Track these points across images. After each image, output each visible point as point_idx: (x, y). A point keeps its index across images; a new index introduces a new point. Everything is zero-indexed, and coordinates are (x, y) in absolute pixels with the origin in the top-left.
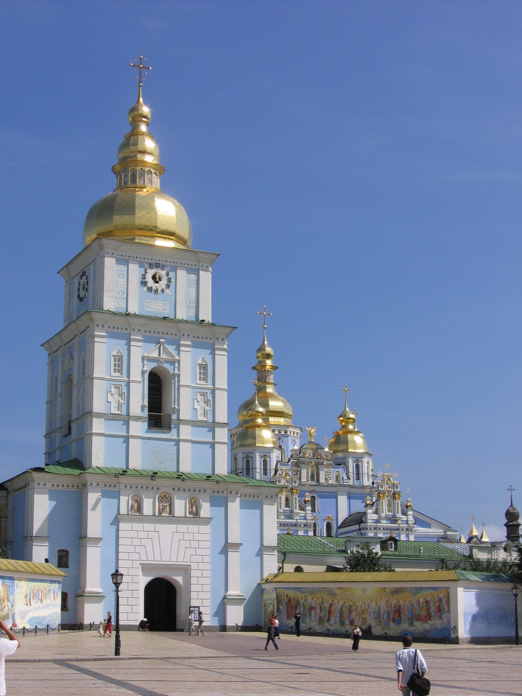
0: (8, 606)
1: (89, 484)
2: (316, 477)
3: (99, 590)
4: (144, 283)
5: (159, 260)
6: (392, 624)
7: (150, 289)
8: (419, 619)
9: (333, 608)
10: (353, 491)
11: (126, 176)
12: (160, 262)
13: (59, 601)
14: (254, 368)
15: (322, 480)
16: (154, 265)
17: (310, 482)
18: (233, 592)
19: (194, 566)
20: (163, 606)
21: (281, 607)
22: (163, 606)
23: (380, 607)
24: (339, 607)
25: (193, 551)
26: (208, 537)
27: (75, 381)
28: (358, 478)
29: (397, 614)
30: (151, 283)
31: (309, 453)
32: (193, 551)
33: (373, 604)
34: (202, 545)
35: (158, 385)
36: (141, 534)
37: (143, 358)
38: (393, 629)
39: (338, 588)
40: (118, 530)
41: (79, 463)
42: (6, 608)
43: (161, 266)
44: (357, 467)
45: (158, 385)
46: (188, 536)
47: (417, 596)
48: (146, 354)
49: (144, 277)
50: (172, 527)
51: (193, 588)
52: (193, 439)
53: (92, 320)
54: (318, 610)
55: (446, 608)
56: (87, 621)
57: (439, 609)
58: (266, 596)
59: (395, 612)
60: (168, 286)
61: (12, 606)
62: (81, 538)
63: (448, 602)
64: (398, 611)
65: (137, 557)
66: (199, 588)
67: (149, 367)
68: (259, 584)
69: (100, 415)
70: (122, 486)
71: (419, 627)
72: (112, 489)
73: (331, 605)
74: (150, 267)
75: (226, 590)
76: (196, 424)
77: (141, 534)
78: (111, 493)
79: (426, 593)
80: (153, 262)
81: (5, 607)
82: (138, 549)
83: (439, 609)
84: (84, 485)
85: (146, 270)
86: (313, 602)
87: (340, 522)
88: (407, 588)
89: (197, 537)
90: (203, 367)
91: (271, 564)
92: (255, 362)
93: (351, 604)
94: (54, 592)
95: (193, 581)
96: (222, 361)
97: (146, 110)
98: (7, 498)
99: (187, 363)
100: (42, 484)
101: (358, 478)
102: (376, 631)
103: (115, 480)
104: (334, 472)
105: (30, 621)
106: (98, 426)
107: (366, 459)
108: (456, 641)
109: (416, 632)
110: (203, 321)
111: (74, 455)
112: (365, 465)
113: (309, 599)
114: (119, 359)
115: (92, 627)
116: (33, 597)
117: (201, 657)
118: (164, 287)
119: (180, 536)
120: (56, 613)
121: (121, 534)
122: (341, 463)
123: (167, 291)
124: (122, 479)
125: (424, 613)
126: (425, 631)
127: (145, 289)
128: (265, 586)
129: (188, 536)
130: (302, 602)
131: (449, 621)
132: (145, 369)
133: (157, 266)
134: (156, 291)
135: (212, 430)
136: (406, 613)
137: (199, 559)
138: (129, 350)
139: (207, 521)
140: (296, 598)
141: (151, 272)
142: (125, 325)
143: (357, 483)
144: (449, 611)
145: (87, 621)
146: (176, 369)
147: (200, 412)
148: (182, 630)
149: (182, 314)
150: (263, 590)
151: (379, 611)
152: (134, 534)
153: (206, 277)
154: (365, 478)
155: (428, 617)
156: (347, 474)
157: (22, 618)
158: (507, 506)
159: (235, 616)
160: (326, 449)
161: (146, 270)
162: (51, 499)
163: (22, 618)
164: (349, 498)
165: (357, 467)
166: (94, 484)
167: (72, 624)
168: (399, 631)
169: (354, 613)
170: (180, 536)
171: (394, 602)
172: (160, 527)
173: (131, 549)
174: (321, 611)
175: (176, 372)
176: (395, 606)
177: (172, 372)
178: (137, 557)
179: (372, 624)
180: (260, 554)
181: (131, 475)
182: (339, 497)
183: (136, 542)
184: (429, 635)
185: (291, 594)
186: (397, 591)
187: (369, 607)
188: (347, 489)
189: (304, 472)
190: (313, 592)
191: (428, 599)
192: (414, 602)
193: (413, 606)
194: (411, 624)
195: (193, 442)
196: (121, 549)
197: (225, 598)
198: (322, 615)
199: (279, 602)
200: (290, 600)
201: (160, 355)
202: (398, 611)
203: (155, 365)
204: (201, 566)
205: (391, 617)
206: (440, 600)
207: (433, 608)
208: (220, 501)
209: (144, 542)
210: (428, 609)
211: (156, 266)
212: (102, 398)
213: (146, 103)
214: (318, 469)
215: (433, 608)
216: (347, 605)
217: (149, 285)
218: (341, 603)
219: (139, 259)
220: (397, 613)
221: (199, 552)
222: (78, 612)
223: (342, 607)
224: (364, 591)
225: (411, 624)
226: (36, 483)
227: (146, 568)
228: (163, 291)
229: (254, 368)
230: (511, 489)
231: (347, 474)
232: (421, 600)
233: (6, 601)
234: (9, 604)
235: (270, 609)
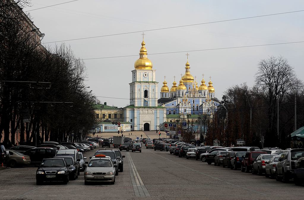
13: (130, 127)
15: (196, 97)
18: (158, 125)
28: (204, 96)
30: (145, 76)
35: (146, 92)
45: (146, 92)
56: (135, 130)
87: (200, 105)
101: (204, 96)
104: (199, 94)
145: (135, 130)
147: (153, 96)
157: (124, 130)
159: (158, 128)
163: (124, 130)
165: (204, 93)
167: (133, 130)
188: (202, 98)
212: (137, 96)
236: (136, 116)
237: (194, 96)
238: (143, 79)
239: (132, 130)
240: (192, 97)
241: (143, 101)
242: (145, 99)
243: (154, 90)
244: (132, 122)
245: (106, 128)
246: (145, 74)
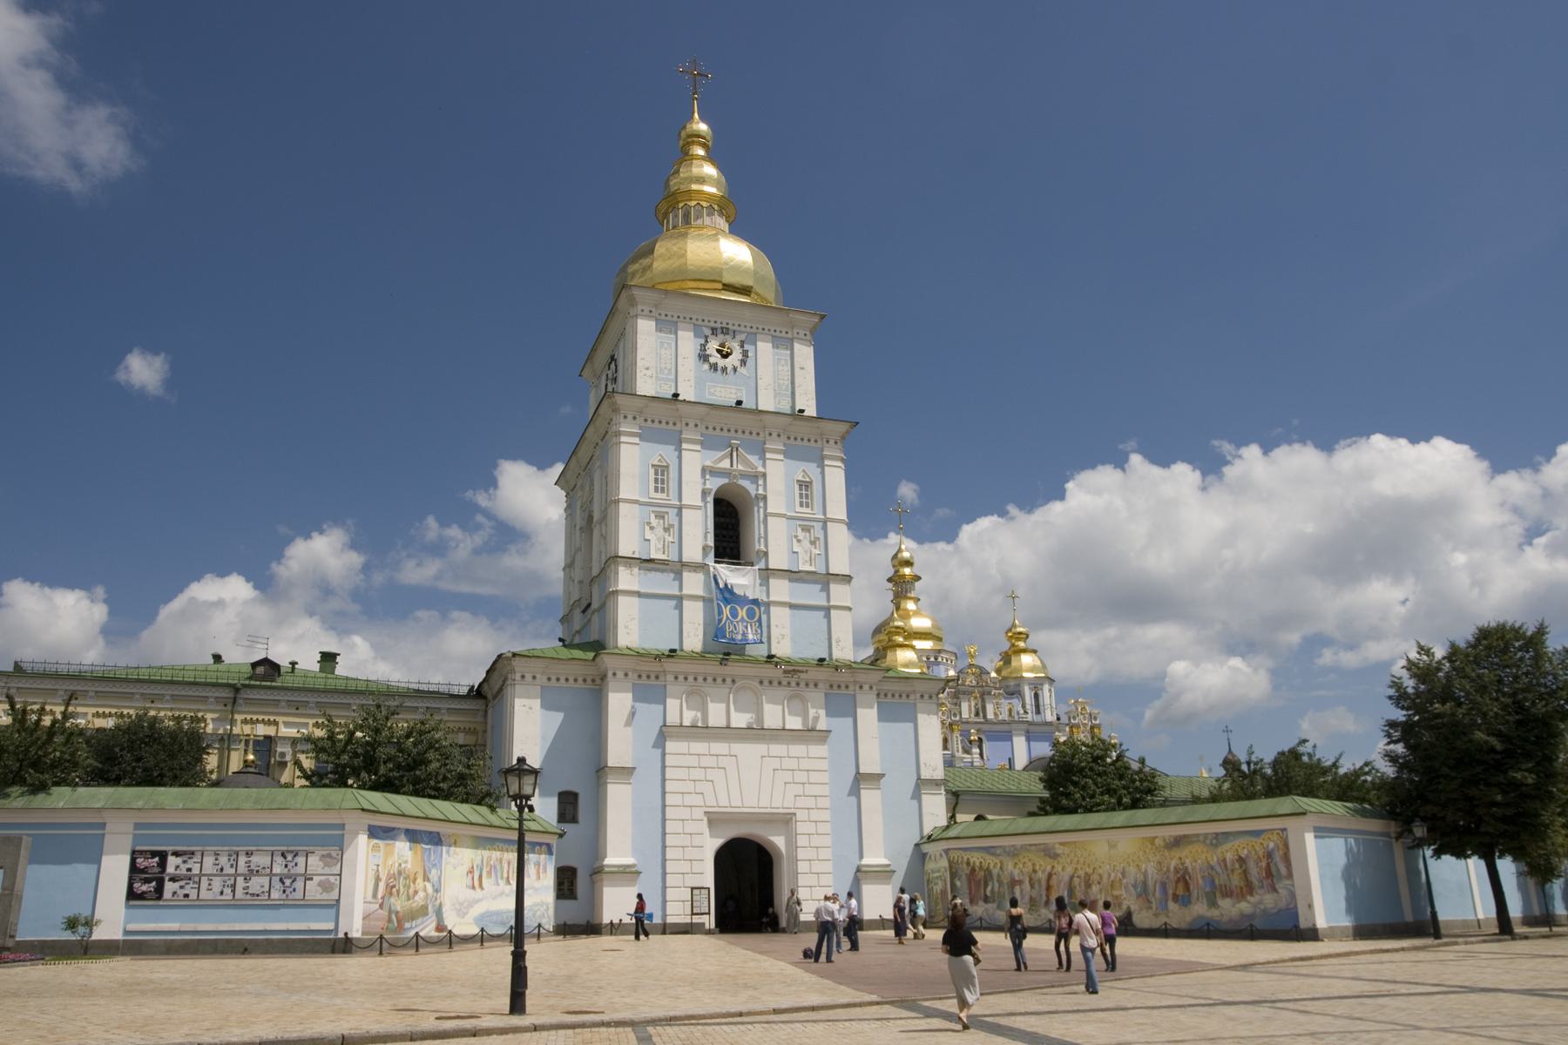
0: (425, 890)
1: (610, 674)
2: (980, 711)
3: (629, 861)
4: (704, 357)
6: (1171, 905)
7: (714, 367)
8: (1228, 893)
9: (1054, 882)
10: (1032, 728)
11: (676, 216)
14: (889, 580)
15: (990, 716)
17: (974, 719)
19: (801, 815)
20: (747, 887)
21: (958, 883)
22: (747, 887)
23: (1145, 874)
24: (1067, 879)
25: (799, 789)
26: (824, 765)
27: (596, 516)
28: (1038, 712)
29: (1181, 886)
30: (716, 358)
31: (970, 680)
32: (799, 789)
33: (1132, 870)
34: (814, 777)
36: (706, 761)
37: (704, 470)
38: (1177, 916)
39: (1062, 844)
40: (664, 755)
41: (598, 646)
42: (421, 894)
44: (1036, 696)
46: (787, 764)
47: (1220, 850)
48: (708, 463)
49: (703, 347)
50: (761, 748)
51: (801, 854)
52: (794, 601)
53: (616, 410)
54: (1027, 885)
55: (1283, 871)
57: (1269, 874)
58: (930, 866)
59: (1178, 881)
60: (743, 362)
61: (437, 891)
62: (600, 772)
63: (1286, 858)
64: (1183, 878)
65: (698, 800)
66: (811, 854)
67: (714, 484)
68: (917, 845)
69: (630, 561)
70: (670, 678)
71: (1229, 909)
72: (653, 682)
73: (1050, 875)
75: (861, 857)
76: (793, 575)
77: (706, 761)
78: (650, 687)
79: (1236, 843)
80: (718, 325)
81: (416, 892)
82: (700, 787)
83: (1269, 874)
84: (603, 678)
86: (1016, 872)
88: (1197, 835)
89: (805, 764)
90: (805, 485)
91: (935, 810)
92: (891, 572)
93: (1090, 871)
94: (538, 864)
95: (801, 841)
96: (836, 477)
97: (703, 127)
98: (486, 711)
99: (777, 482)
100: (528, 677)
101: (1038, 712)
102: (1142, 919)
103: (655, 667)
104: (1005, 704)
105: (477, 920)
106: (626, 579)
107: (1046, 687)
108: (1312, 935)
109: (1225, 919)
110: (802, 411)
111: (594, 637)
112: (1046, 693)
113: (1010, 866)
114: (661, 470)
115: (614, 929)
116: (489, 873)
117: (776, 1011)
118: (737, 364)
119: (776, 763)
120: (542, 904)
121: (669, 760)
122: (1014, 692)
123: (742, 370)
124: (670, 665)
125: (1236, 881)
126: (1243, 916)
127: (706, 366)
128: (927, 848)
129: (787, 764)
130: (995, 872)
131: (1293, 895)
133: (725, 331)
134: (724, 369)
135: (826, 589)
136: (1198, 883)
137: (810, 802)
138: (680, 457)
139: (823, 736)
140: (985, 865)
141: (713, 346)
142: (670, 418)
143: (1037, 719)
144: (1290, 875)
147: (803, 557)
148: (784, 931)
149: (767, 403)
150: (924, 855)
151: (1145, 883)
152: (693, 761)
153: (805, 354)
154: (1048, 712)
155: (1249, 888)
156: (1024, 706)
157: (461, 913)
158: (1223, 753)
159: (878, 902)
160: (993, 675)
162: (546, 706)
163: (461, 913)
164: (1028, 740)
165: (1036, 696)
166: (620, 674)
168: (1188, 919)
169: (1095, 888)
170: (776, 763)
171: (1173, 863)
172: (738, 748)
173: (690, 787)
174: (1032, 887)
175: (761, 491)
176: (1177, 870)
177: (753, 493)
178: (698, 800)
179: (1133, 908)
180: (917, 796)
181: (682, 657)
182: (1015, 739)
183: (697, 774)
184: (1259, 924)
185: (976, 859)
186: (1178, 842)
187: (1123, 874)
188: (1025, 726)
189: (965, 706)
190: (1013, 853)
191: (1244, 853)
192: (1214, 861)
193: (1212, 868)
194: (1213, 904)
195: (792, 606)
196: (669, 786)
197: (858, 870)
198: (1034, 893)
199: (953, 875)
200: (973, 870)
202: (1183, 878)
203: (726, 481)
204: (815, 815)
205: (1170, 892)
206: (1269, 855)
207: (1255, 872)
208: (841, 705)
209: (711, 774)
210: (1245, 872)
213: (703, 119)
214: (983, 701)
215: (1255, 872)
216: (1081, 873)
217: (712, 360)
218: (1070, 870)
220: (1181, 885)
221: (810, 790)
222: (594, 902)
223: (1072, 878)
224: (1112, 846)
225: (1213, 904)
226: (518, 676)
227: (715, 820)
228: (735, 369)
229: (889, 580)
230: (1227, 731)
231: (1024, 706)
232: (1229, 856)
233: (420, 881)
234: (429, 886)
235: (938, 888)
236: (619, 750)
237: (977, 714)
238: (700, 384)
239: (574, 912)
240: (965, 715)
241: (694, 583)
242: (730, 575)
243: (816, 487)
244: (574, 820)
245: (147, 882)
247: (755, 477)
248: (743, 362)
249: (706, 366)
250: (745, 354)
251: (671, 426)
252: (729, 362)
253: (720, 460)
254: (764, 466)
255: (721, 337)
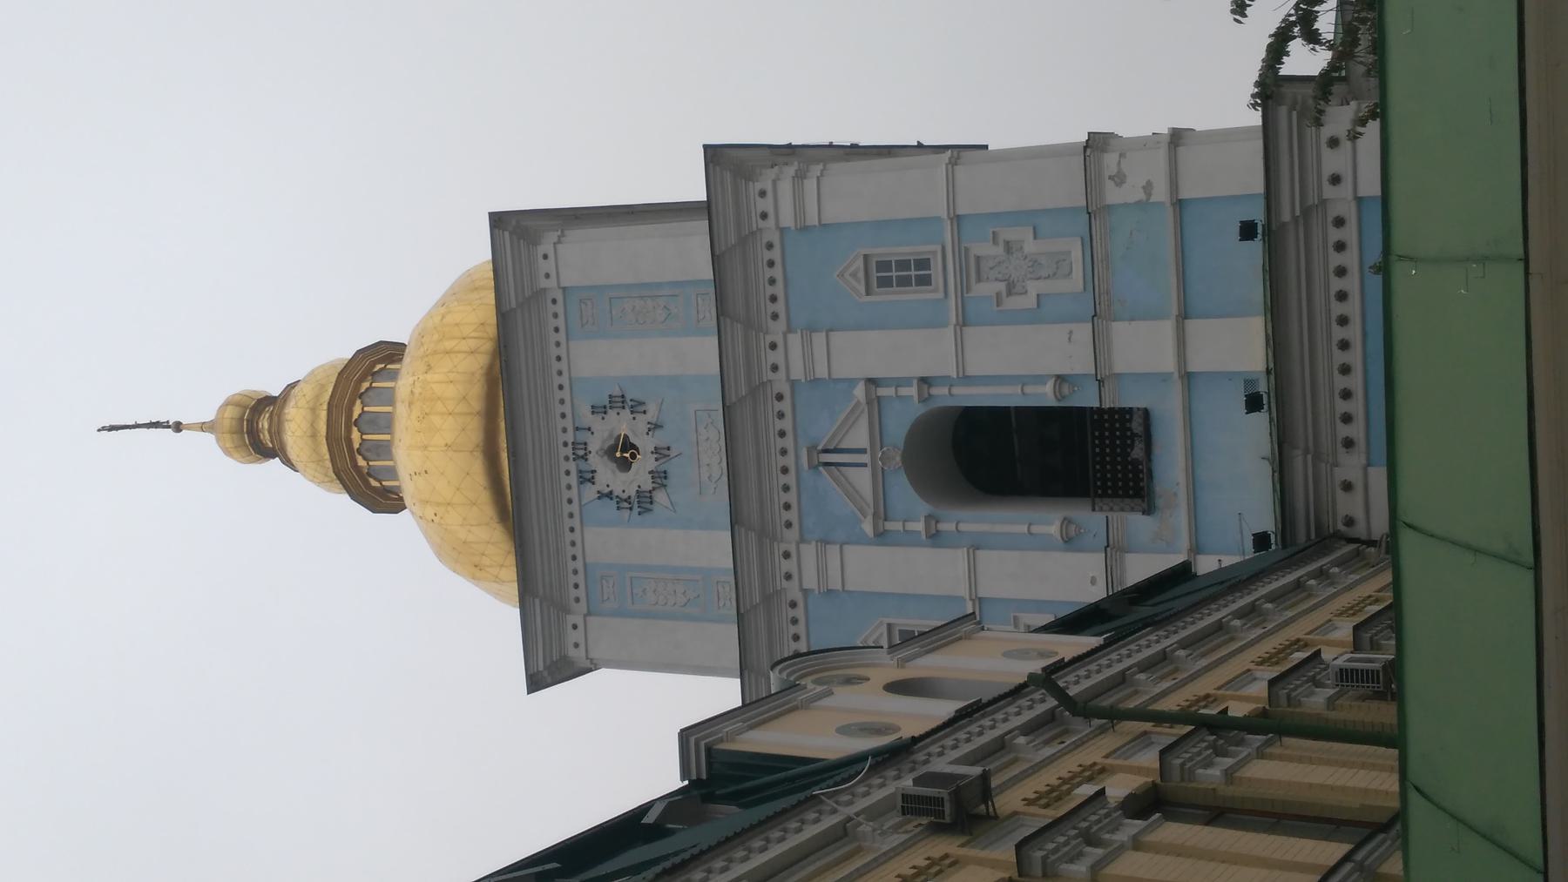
4: (643, 502)
5: (565, 444)
12: (570, 438)
16: (583, 465)
30: (639, 476)
37: (881, 537)
43: (582, 436)
48: (868, 527)
49: (623, 502)
60: (637, 407)
74: (592, 481)
80: (572, 466)
85: (601, 495)
118: (642, 422)
132: (919, 526)
133: (580, 452)
134: (661, 453)
146: (904, 391)
161: (601, 495)
175: (913, 391)
177: (917, 410)
201: (865, 465)
211: (585, 458)
219: (576, 522)
228: (655, 427)
246: (608, 476)
247: (876, 405)
248: (637, 407)
249: (660, 496)
250: (618, 402)
251: (799, 612)
252: (645, 443)
253: (852, 493)
254: (852, 382)
255: (597, 462)
